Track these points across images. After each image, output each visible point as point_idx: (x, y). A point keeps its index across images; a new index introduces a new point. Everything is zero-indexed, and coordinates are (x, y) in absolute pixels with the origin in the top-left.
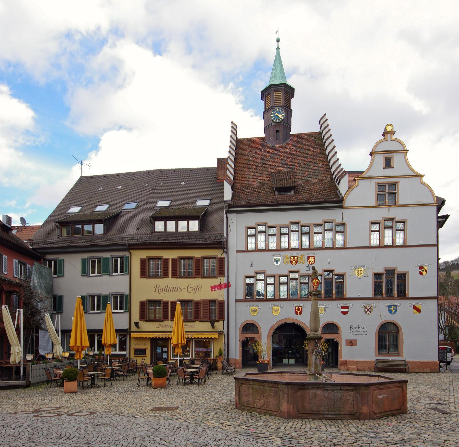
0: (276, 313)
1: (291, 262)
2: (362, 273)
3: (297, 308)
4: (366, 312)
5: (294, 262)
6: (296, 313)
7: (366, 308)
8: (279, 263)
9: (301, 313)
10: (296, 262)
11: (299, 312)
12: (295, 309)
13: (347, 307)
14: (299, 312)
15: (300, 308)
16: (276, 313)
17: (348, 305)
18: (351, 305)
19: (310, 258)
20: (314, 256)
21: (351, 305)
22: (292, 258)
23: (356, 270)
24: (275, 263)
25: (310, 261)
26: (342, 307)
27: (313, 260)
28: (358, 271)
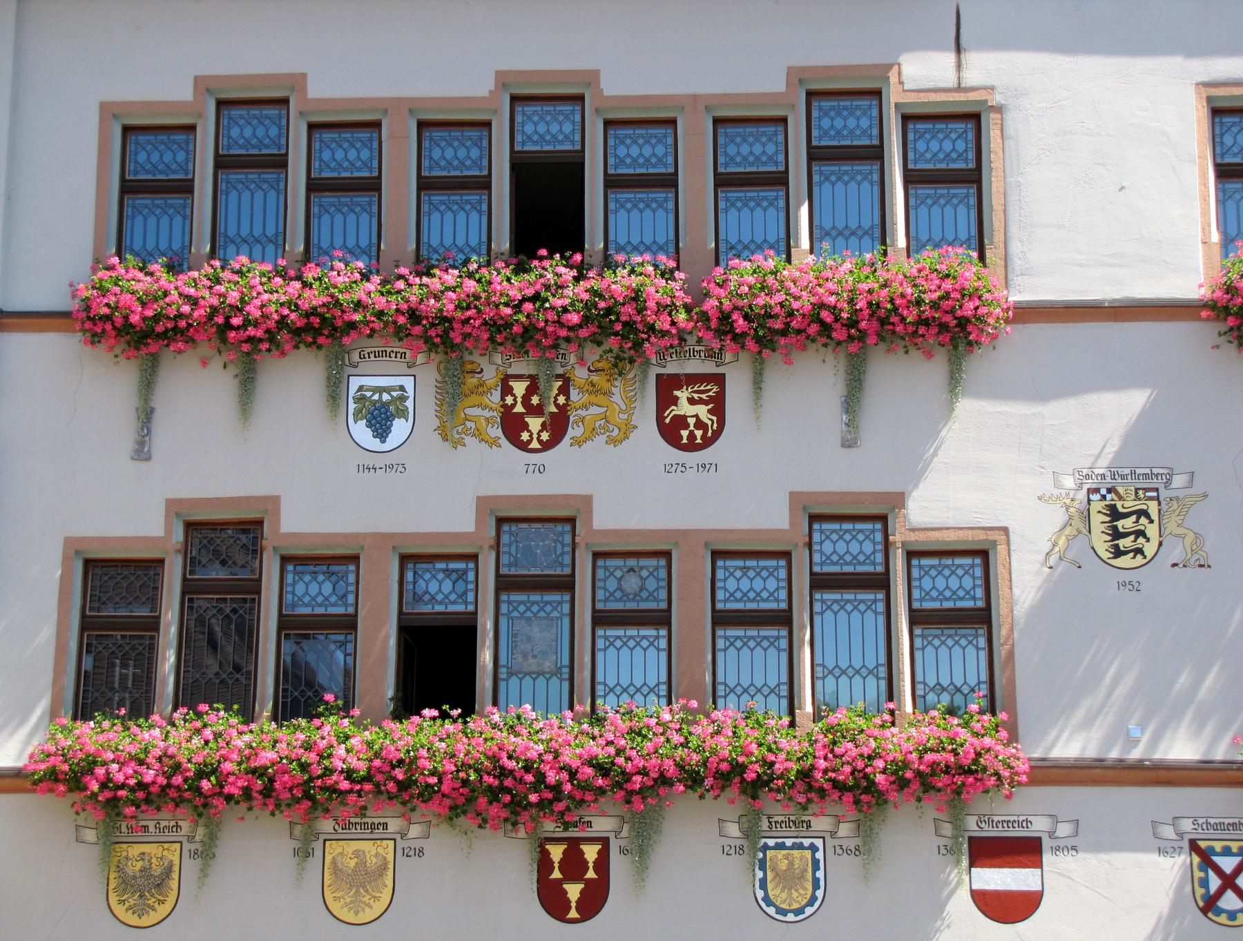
0: (356, 906)
1: (512, 426)
2: (1152, 531)
3: (556, 852)
4: (1209, 905)
5: (535, 423)
6: (553, 902)
7: (1207, 860)
8: (400, 429)
9: (593, 902)
10: (558, 426)
11: (573, 891)
12: (544, 864)
13: (1026, 851)
14: (573, 891)
15: (591, 852)
16: (356, 906)
17: (1039, 826)
18: (1064, 830)
19: (683, 395)
20: (719, 380)
21: (1064, 830)
22: (520, 388)
23: (1097, 505)
24: (362, 432)
25: (681, 421)
26: (986, 851)
27: (702, 411)
28: (1115, 514)
